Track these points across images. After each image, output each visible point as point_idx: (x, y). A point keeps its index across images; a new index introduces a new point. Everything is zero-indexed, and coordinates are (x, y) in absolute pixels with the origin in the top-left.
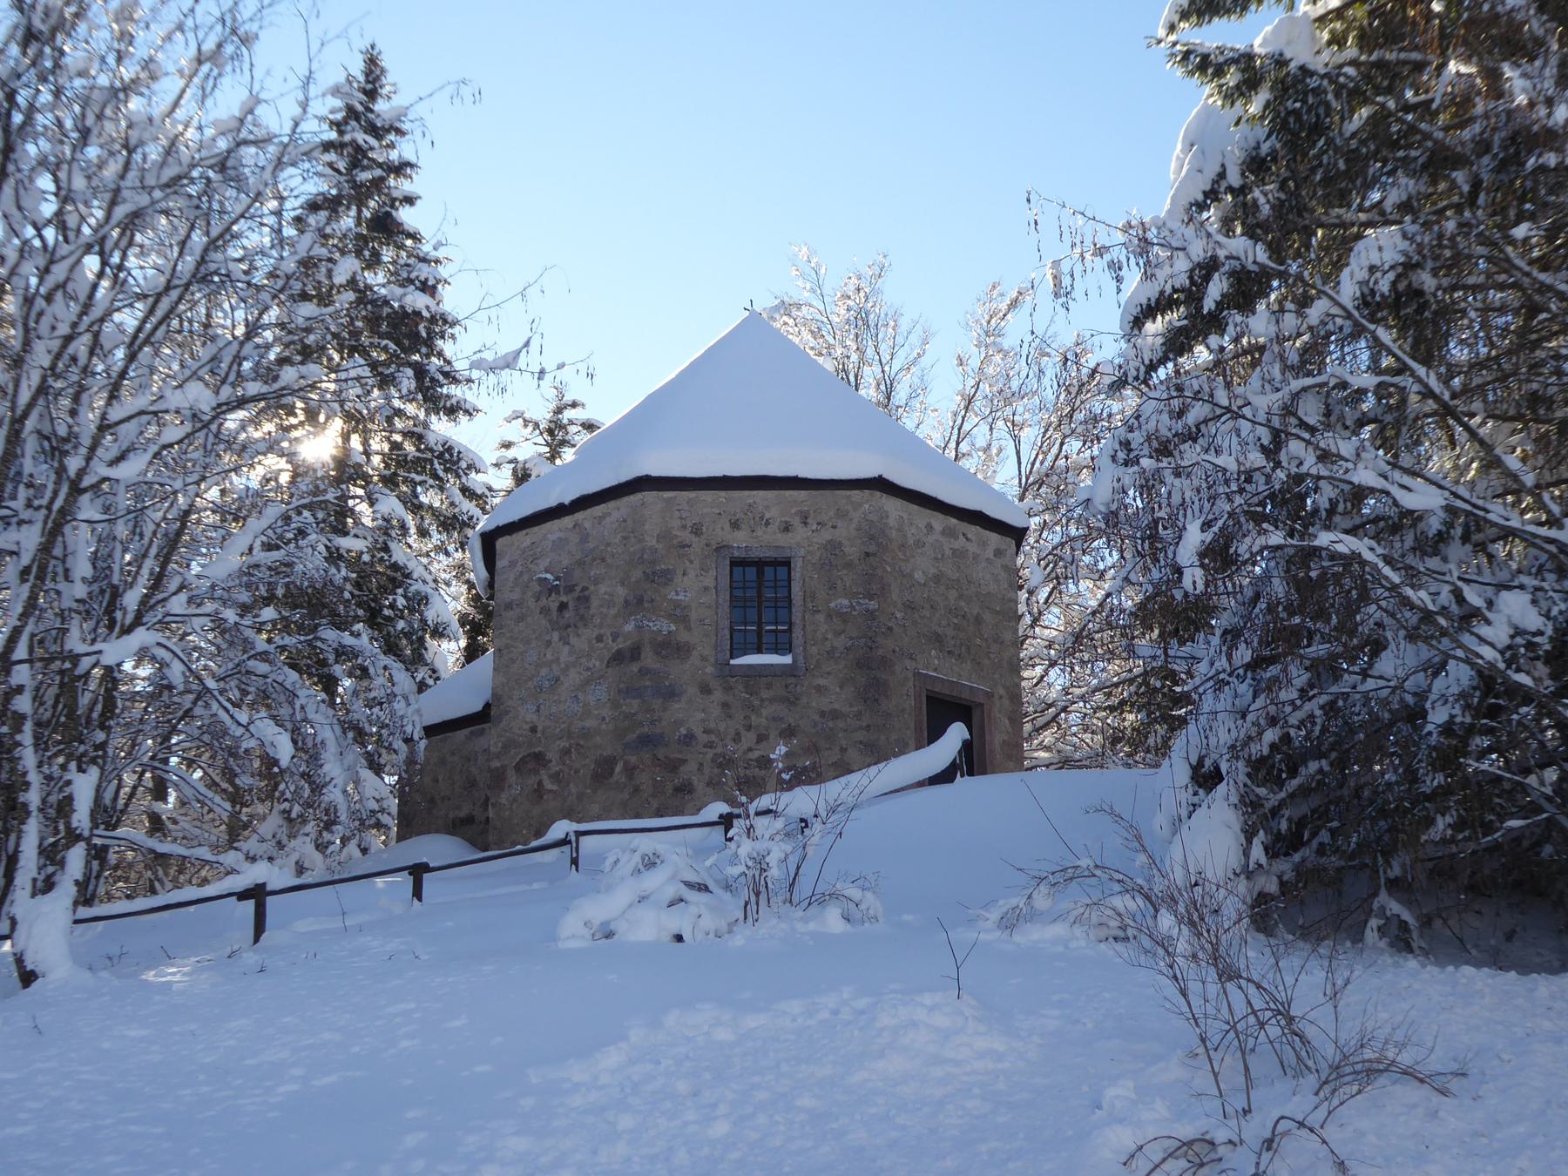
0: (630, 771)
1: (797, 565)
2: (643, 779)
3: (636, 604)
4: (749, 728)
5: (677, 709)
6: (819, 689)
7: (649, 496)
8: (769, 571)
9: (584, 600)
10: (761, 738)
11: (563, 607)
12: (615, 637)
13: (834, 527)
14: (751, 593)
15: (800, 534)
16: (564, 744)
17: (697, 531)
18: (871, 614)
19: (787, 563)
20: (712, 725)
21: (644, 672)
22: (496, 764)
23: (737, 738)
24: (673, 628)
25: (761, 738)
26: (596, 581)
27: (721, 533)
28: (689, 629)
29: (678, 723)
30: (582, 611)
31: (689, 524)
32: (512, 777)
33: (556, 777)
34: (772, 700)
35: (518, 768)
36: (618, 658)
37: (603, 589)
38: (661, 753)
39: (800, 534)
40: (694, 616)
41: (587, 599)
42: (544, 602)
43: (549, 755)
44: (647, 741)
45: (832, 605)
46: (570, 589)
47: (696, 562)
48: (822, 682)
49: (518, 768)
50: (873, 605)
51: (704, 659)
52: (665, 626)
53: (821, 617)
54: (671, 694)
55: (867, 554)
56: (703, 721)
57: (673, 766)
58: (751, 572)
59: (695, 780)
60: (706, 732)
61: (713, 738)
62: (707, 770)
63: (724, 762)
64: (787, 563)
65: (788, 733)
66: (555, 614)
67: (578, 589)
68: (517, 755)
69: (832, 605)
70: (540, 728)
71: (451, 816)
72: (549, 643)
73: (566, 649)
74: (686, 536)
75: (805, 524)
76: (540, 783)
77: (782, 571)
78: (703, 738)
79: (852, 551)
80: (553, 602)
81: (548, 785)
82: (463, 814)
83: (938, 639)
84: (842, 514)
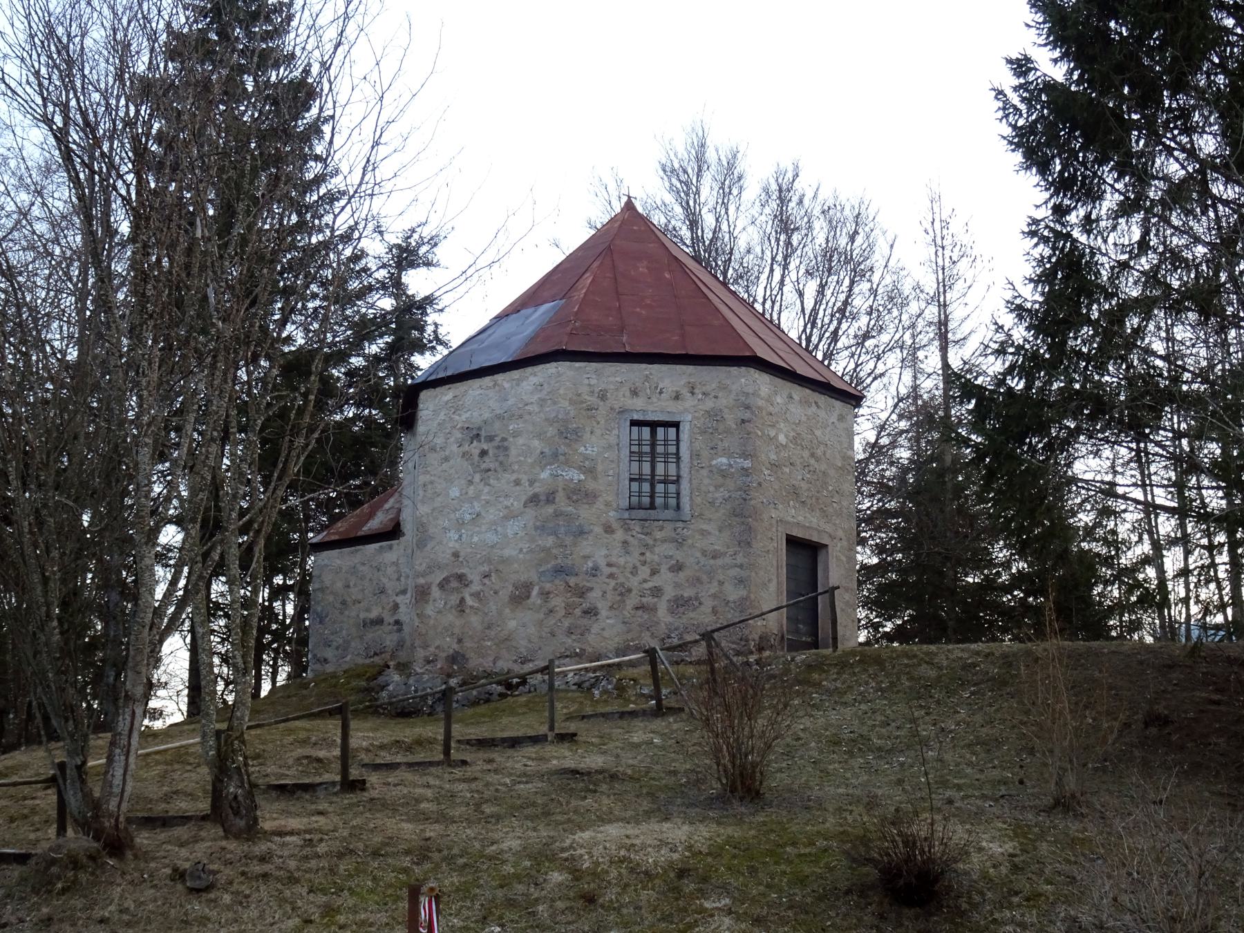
0: (545, 595)
1: (685, 429)
2: (558, 602)
4: (644, 563)
5: (585, 547)
6: (704, 533)
8: (660, 431)
9: (503, 448)
10: (654, 572)
11: (483, 453)
12: (532, 483)
13: (716, 397)
14: (647, 449)
15: (689, 402)
16: (486, 568)
17: (603, 396)
18: (745, 472)
19: (676, 425)
20: (614, 560)
21: (557, 514)
22: (421, 581)
23: (634, 571)
24: (582, 477)
25: (654, 572)
26: (516, 434)
28: (595, 479)
29: (586, 557)
30: (501, 458)
31: (597, 390)
32: (436, 592)
33: (476, 595)
34: (664, 541)
35: (441, 586)
36: (534, 500)
37: (521, 441)
38: (572, 581)
39: (689, 402)
40: (600, 468)
41: (506, 449)
42: (466, 447)
43: (470, 577)
44: (559, 571)
45: (714, 462)
46: (490, 439)
47: (603, 422)
48: (705, 527)
49: (441, 586)
50: (747, 464)
51: (607, 504)
52: (576, 476)
53: (705, 472)
54: (581, 533)
55: (743, 421)
56: (607, 556)
57: (582, 593)
58: (646, 431)
59: (599, 605)
60: (609, 565)
61: (614, 570)
62: (609, 596)
63: (624, 592)
64: (676, 425)
65: (678, 568)
66: (476, 458)
67: (498, 439)
68: (438, 577)
69: (714, 462)
70: (462, 554)
71: (362, 616)
72: (471, 482)
73: (486, 489)
74: (593, 400)
75: (693, 393)
76: (462, 600)
77: (672, 431)
79: (731, 419)
80: (475, 448)
81: (470, 601)
82: (374, 614)
83: (795, 492)
84: (723, 387)
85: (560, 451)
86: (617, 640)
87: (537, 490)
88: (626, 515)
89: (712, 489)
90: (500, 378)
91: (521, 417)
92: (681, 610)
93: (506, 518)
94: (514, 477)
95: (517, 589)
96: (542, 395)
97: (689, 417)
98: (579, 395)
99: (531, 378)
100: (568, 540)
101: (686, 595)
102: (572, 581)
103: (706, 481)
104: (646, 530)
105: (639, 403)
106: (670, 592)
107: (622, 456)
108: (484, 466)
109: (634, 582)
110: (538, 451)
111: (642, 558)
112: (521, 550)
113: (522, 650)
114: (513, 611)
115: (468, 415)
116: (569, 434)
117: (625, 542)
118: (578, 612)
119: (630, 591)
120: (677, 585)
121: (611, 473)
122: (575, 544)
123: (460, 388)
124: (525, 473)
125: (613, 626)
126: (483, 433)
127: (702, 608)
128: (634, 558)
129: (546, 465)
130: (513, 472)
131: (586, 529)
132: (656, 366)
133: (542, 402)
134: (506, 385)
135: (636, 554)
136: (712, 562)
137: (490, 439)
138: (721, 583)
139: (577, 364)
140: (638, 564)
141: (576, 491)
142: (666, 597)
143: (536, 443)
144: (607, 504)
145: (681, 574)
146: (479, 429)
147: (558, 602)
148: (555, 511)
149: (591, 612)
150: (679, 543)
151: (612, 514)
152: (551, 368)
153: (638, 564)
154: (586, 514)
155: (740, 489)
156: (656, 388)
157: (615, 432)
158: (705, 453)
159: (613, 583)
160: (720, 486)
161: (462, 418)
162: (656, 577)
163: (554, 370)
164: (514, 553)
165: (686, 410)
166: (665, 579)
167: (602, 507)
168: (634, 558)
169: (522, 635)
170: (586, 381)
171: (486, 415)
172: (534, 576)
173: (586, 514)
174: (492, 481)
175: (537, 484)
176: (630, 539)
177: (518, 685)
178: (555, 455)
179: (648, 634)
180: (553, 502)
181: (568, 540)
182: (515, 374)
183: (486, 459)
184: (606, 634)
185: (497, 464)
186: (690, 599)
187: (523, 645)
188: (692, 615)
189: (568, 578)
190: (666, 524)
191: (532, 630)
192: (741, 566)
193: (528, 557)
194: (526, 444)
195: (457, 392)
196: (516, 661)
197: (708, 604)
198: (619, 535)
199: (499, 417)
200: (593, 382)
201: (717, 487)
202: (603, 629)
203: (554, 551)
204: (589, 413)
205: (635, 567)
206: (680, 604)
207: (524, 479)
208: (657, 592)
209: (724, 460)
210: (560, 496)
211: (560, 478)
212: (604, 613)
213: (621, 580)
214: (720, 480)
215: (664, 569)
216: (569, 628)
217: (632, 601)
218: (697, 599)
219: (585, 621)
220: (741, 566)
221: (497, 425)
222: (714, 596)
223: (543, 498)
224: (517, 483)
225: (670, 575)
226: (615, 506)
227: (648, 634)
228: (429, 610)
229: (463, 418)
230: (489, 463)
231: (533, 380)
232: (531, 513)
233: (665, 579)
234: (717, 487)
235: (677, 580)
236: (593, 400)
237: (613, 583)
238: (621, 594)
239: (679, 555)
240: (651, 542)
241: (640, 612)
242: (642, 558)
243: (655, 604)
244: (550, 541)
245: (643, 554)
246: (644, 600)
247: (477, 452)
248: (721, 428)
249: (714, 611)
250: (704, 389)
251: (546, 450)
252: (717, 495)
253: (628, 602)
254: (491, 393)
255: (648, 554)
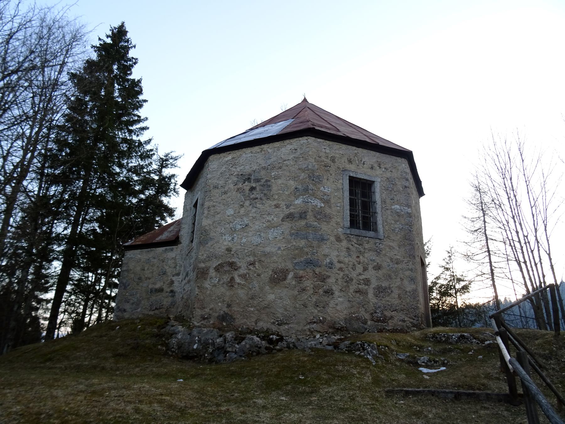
0: (299, 279)
2: (308, 284)
3: (296, 192)
5: (325, 249)
6: (391, 248)
7: (311, 140)
9: (267, 185)
10: (365, 269)
11: (252, 189)
12: (288, 207)
13: (391, 171)
16: (251, 259)
20: (342, 259)
21: (308, 226)
22: (202, 265)
23: (354, 268)
24: (323, 205)
25: (365, 269)
26: (277, 178)
27: (343, 163)
28: (330, 207)
29: (326, 256)
30: (266, 192)
31: (330, 156)
32: (212, 272)
33: (243, 276)
34: (370, 250)
35: (217, 269)
36: (290, 217)
37: (280, 181)
38: (317, 270)
39: (379, 172)
40: (332, 201)
43: (239, 264)
44: (309, 263)
45: (393, 207)
46: (258, 180)
47: (333, 175)
48: (391, 244)
49: (217, 269)
51: (337, 224)
52: (320, 204)
53: (389, 212)
54: (322, 239)
55: (406, 187)
56: (338, 256)
57: (324, 279)
59: (334, 288)
60: (339, 262)
61: (342, 265)
62: (340, 283)
65: (378, 268)
66: (247, 192)
67: (263, 181)
68: (215, 263)
69: (393, 207)
70: (234, 249)
71: (150, 286)
73: (254, 210)
74: (328, 161)
75: (380, 168)
76: (232, 279)
78: (338, 265)
80: (247, 186)
81: (238, 280)
82: (158, 286)
85: (310, 187)
86: (345, 312)
87: (292, 211)
88: (348, 232)
89: (393, 222)
90: (265, 147)
91: (280, 168)
92: (382, 294)
93: (268, 228)
94: (275, 202)
95: (275, 273)
96: (297, 155)
97: (379, 180)
98: (320, 157)
99: (288, 146)
100: (315, 243)
101: (383, 285)
102: (317, 270)
103: (390, 217)
104: (359, 242)
105: (352, 167)
106: (374, 283)
107: (345, 196)
108: (252, 196)
109: (354, 275)
110: (293, 187)
111: (358, 260)
112: (279, 248)
113: (279, 315)
114: (272, 288)
115: (242, 167)
116: (315, 178)
117: (348, 248)
118: (321, 291)
119: (352, 280)
120: (378, 279)
121: (339, 205)
122: (319, 247)
123: (237, 153)
124: (283, 200)
125: (342, 303)
126: (252, 177)
127: (393, 295)
128: (353, 259)
129: (299, 196)
130: (274, 199)
131: (325, 238)
132: (360, 149)
133: (296, 159)
134: (270, 151)
135: (354, 257)
136: (396, 266)
137: (258, 180)
138: (402, 280)
139: (319, 140)
140: (356, 263)
141: (320, 213)
142: (373, 286)
143: (292, 182)
144: (337, 224)
145: (380, 272)
146: (250, 175)
147: (308, 284)
148: (307, 224)
149: (329, 292)
150: (378, 252)
151: (340, 230)
152: (303, 140)
153: (356, 263)
154: (325, 228)
155: (407, 224)
156: (361, 161)
157: (341, 181)
158: (388, 201)
159: (342, 274)
160: (397, 221)
161: (238, 170)
162: (366, 272)
163: (305, 141)
164: (274, 250)
165: (377, 176)
166: (371, 274)
167: (334, 225)
168: (353, 259)
169: (278, 305)
170: (324, 150)
171: (255, 167)
172: (290, 266)
173: (325, 228)
174: (258, 205)
175: (292, 207)
176: (351, 247)
177: (278, 341)
178: (306, 190)
179: (363, 309)
180: (305, 218)
181: (315, 243)
182: (277, 144)
183: (255, 192)
184: (338, 308)
185: (262, 195)
186: (386, 288)
187: (280, 312)
188: (388, 298)
189: (315, 268)
190: (370, 240)
191: (287, 302)
192: (411, 270)
193: (285, 253)
194: (283, 184)
195: (235, 155)
196: (274, 323)
197: (396, 292)
198: (344, 243)
199: (264, 168)
200: (328, 151)
201: (396, 221)
202: (337, 305)
203: (306, 249)
204: (326, 169)
205: (354, 265)
206: (380, 291)
207: (283, 204)
208: (367, 282)
209: (398, 207)
210: (310, 215)
211: (310, 204)
212: (337, 293)
213: (347, 272)
214: (397, 218)
215: (370, 267)
216: (316, 302)
217: (353, 288)
218: (390, 288)
219: (326, 298)
220: (411, 270)
221: (263, 173)
222: (399, 287)
223: (298, 215)
224: (277, 206)
225: (374, 272)
226: (342, 225)
227: (363, 309)
228: (207, 284)
229: (238, 169)
230: (255, 194)
231: (289, 147)
232: (287, 226)
233: (371, 274)
234: (396, 221)
235: (377, 275)
236: (328, 161)
237: (342, 274)
238: (347, 282)
239: (378, 260)
240: (362, 250)
241: (358, 295)
242: (358, 260)
243: (366, 290)
244: (303, 243)
245: (358, 257)
246: (360, 286)
247: (248, 188)
248: (395, 189)
249: (400, 297)
250: (385, 166)
251: (300, 187)
252: (396, 226)
253: (351, 287)
254: (259, 155)
255: (361, 257)
